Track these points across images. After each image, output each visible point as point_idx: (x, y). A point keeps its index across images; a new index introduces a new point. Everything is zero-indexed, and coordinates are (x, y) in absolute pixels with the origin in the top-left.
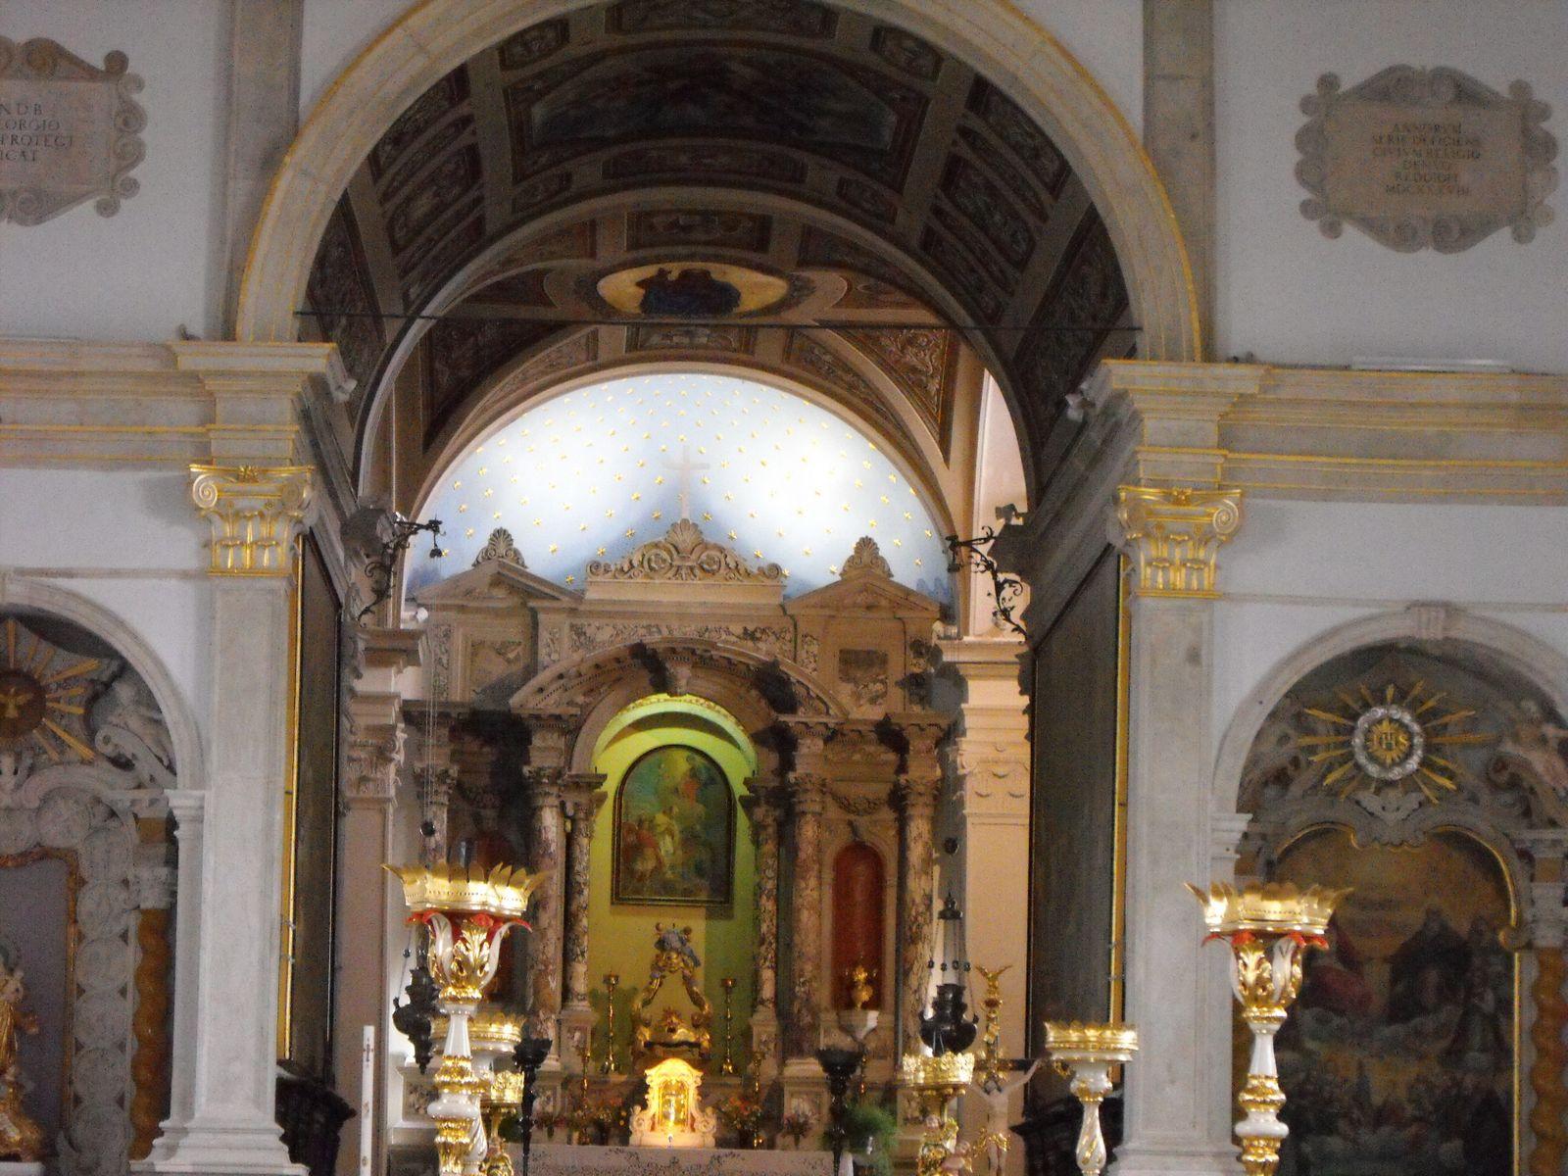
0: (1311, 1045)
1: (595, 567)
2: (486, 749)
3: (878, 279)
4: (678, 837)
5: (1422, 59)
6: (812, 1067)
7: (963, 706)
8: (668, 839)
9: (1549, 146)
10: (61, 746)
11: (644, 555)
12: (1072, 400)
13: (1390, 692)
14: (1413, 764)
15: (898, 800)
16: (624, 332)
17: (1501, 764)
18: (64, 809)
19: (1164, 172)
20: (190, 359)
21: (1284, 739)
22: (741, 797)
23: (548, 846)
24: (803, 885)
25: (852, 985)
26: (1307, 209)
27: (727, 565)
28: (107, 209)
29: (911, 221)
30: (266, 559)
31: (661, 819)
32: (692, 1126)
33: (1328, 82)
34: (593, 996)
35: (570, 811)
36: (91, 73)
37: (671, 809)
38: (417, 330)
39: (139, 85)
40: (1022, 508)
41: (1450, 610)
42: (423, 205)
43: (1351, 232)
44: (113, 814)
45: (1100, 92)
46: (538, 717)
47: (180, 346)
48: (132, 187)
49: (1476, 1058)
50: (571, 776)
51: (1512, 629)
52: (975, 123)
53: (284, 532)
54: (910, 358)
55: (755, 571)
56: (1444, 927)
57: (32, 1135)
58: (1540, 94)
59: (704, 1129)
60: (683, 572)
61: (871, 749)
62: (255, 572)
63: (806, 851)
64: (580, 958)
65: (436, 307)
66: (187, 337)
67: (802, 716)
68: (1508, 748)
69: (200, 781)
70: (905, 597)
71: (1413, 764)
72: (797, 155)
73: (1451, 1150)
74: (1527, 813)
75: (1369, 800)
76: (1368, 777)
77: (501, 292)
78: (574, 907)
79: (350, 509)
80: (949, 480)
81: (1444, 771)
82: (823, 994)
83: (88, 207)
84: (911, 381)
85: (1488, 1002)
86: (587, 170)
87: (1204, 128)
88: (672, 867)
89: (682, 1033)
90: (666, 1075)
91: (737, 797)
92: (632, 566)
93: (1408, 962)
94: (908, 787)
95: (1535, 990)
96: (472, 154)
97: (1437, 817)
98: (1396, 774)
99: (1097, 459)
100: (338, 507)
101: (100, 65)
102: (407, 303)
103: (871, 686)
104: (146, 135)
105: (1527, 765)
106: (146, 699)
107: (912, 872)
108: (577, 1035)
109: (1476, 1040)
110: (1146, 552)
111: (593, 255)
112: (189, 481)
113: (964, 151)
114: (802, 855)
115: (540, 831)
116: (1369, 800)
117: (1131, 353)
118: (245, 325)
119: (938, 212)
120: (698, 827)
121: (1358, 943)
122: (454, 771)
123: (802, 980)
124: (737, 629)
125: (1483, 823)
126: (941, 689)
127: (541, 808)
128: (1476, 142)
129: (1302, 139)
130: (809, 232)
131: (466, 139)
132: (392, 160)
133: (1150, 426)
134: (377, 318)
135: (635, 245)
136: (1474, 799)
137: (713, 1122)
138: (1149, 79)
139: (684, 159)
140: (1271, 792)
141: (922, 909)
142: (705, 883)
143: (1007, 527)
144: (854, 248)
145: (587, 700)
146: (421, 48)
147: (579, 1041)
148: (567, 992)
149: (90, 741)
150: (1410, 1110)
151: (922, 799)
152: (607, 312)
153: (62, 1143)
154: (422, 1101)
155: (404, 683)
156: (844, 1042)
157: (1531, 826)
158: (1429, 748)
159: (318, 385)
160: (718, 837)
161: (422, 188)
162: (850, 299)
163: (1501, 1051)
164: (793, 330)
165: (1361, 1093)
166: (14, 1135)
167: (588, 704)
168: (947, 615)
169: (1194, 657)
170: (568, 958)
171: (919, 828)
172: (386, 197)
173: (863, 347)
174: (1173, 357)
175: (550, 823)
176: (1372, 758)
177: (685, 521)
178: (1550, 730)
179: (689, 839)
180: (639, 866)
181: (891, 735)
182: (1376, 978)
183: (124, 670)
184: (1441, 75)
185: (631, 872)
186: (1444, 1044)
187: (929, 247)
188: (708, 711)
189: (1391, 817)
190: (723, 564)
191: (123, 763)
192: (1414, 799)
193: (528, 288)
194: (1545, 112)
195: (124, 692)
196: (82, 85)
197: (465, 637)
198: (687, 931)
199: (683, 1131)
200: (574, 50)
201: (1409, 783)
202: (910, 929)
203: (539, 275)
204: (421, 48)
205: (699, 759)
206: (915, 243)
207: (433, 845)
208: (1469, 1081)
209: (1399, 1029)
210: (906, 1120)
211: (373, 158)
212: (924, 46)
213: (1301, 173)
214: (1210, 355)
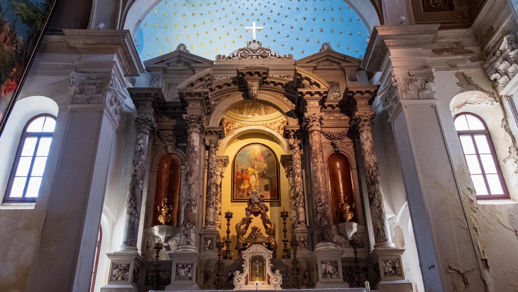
1: (219, 57)
2: (172, 120)
4: (257, 175)
7: (390, 57)
8: (253, 176)
11: (238, 53)
22: (282, 156)
23: (193, 147)
24: (316, 160)
27: (272, 55)
31: (250, 170)
32: (268, 280)
35: (208, 143)
37: (254, 166)
46: (191, 95)
50: (208, 128)
55: (283, 56)
59: (276, 283)
60: (254, 57)
61: (337, 115)
64: (211, 206)
78: (209, 184)
88: (255, 187)
90: (252, 253)
91: (279, 159)
92: (234, 56)
94: (360, 118)
103: (334, 93)
107: (367, 153)
108: (209, 242)
114: (314, 148)
115: (190, 142)
120: (265, 172)
123: (320, 204)
127: (191, 133)
137: (280, 278)
141: (374, 169)
142: (268, 193)
145: (216, 103)
147: (210, 245)
151: (366, 123)
154: (120, 273)
160: (274, 175)
167: (216, 104)
175: (195, 139)
177: (254, 41)
179: (262, 176)
180: (242, 187)
185: (240, 189)
188: (267, 128)
190: (270, 55)
197: (166, 82)
199: (263, 284)
202: (370, 178)
205: (264, 148)
207: (139, 149)
210: (385, 273)
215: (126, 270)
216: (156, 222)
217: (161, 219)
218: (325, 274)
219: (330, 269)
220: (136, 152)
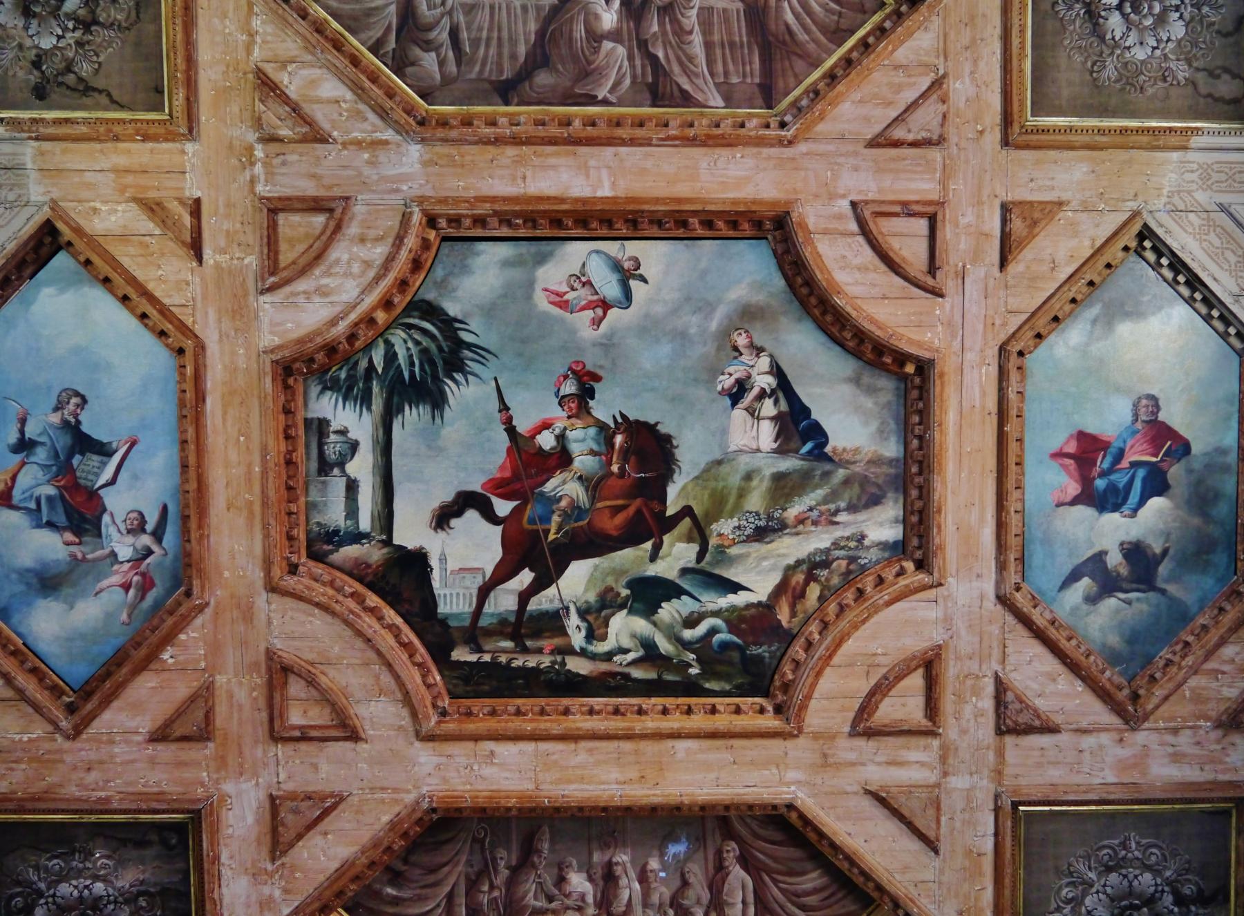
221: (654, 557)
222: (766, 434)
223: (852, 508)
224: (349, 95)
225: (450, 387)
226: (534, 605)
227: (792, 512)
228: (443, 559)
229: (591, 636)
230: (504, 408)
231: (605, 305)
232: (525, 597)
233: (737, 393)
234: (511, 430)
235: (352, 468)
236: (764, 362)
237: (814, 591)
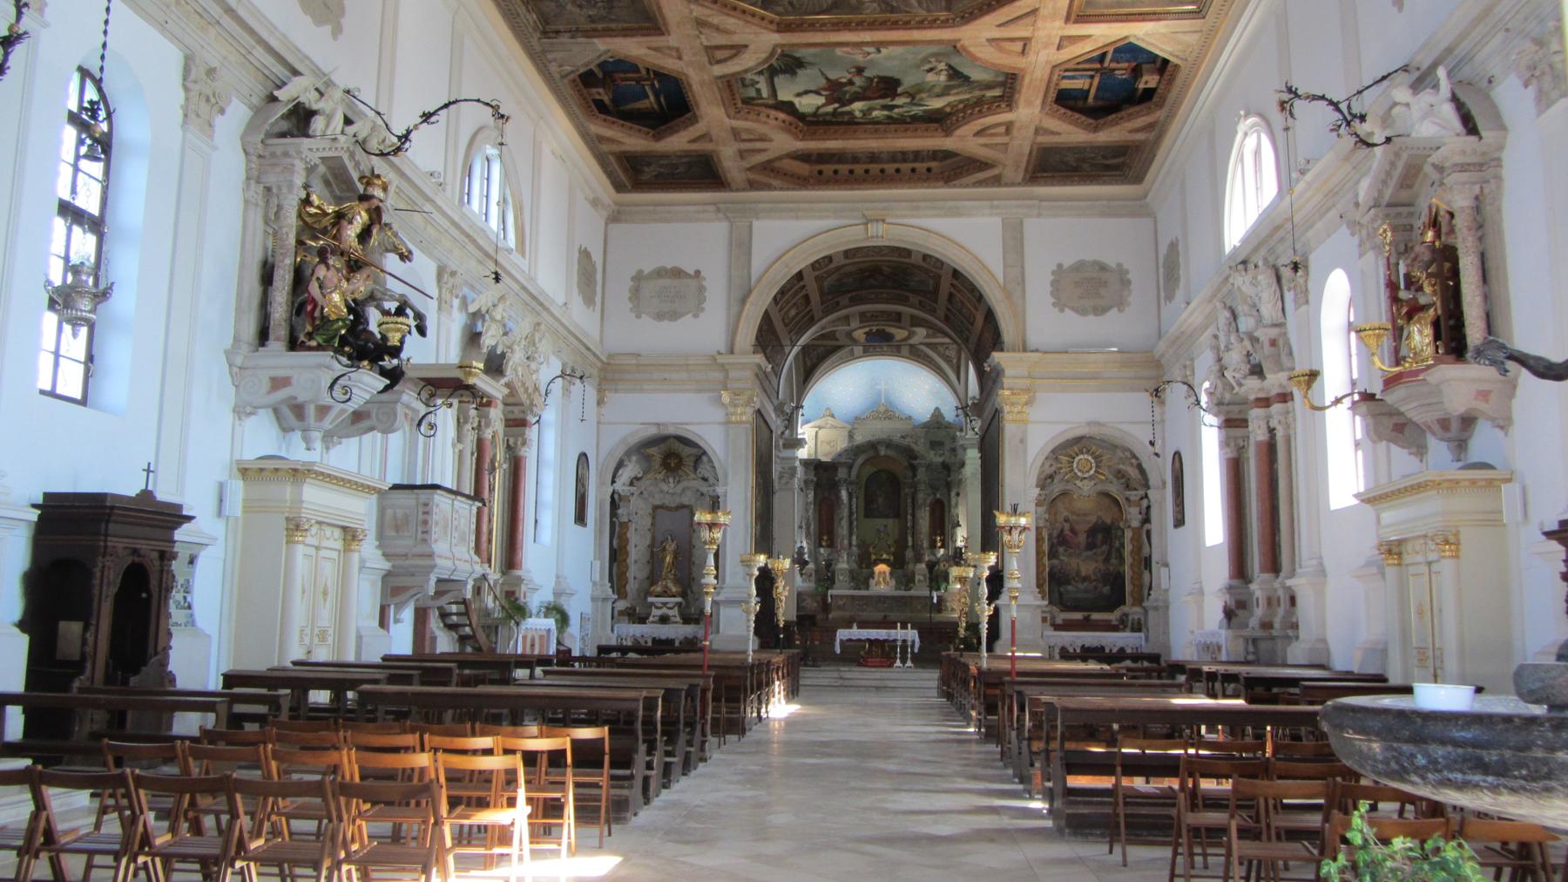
0: (1062, 558)
3: (934, 330)
5: (1088, 256)
6: (923, 566)
9: (1129, 282)
10: (687, 475)
12: (985, 365)
13: (1085, 450)
14: (1092, 472)
15: (949, 486)
16: (861, 348)
17: (1119, 471)
18: (689, 493)
19: (1008, 296)
20: (720, 360)
21: (1051, 465)
25: (935, 541)
26: (1054, 305)
28: (696, 316)
29: (941, 312)
30: (744, 418)
33: (1060, 266)
34: (858, 546)
36: (690, 276)
38: (796, 350)
39: (705, 279)
40: (978, 397)
41: (1099, 424)
42: (793, 312)
43: (1067, 310)
44: (702, 494)
45: (989, 272)
47: (718, 357)
48: (703, 310)
49: (1113, 561)
51: (1121, 430)
52: (955, 282)
53: (750, 411)
54: (947, 353)
56: (1103, 523)
57: (680, 590)
58: (1125, 267)
62: (741, 422)
63: (920, 501)
65: (803, 340)
66: (719, 353)
67: (918, 461)
68: (1121, 466)
69: (726, 484)
70: (948, 426)
71: (1092, 472)
72: (907, 294)
73: (1106, 590)
74: (1128, 486)
75: (1078, 483)
76: (1077, 477)
77: (823, 337)
79: (776, 402)
80: (960, 389)
81: (1102, 474)
82: (926, 544)
83: (690, 315)
84: (947, 360)
85: (1117, 544)
86: (844, 300)
87: (1022, 282)
89: (885, 556)
93: (1092, 531)
95: (1132, 540)
96: (807, 297)
97: (1100, 488)
98: (1086, 475)
99: (994, 382)
100: (772, 402)
101: (693, 274)
102: (792, 342)
104: (706, 294)
105: (1126, 472)
106: (710, 461)
109: (1114, 555)
110: (1007, 409)
111: (849, 325)
112: (721, 396)
113: (954, 292)
116: (1078, 483)
117: (1002, 350)
118: (737, 349)
119: (948, 309)
121: (1077, 528)
122: (815, 479)
124: (899, 435)
125: (1115, 489)
126: (960, 451)
128: (1106, 282)
129: (1053, 283)
130: (912, 317)
131: (804, 292)
132: (781, 299)
133: (1008, 372)
134: (782, 346)
135: (861, 322)
136: (1111, 482)
138: (1005, 267)
139: (873, 296)
140: (1049, 481)
143: (973, 404)
144: (927, 321)
146: (787, 266)
148: (850, 544)
149: (695, 473)
150: (1093, 577)
152: (855, 342)
153: (689, 592)
155: (803, 453)
156: (933, 558)
157: (1130, 490)
158: (1097, 466)
159: (759, 366)
161: (792, 307)
162: (928, 336)
163: (1121, 559)
164: (911, 346)
165: (1078, 573)
166: (674, 590)
168: (961, 430)
169: (1022, 441)
170: (851, 534)
171: (953, 494)
172: (780, 311)
173: (932, 349)
174: (1014, 351)
175: (844, 494)
176: (1080, 470)
178: (1134, 461)
181: (946, 467)
182: (1082, 538)
183: (704, 453)
184: (1096, 263)
186: (1103, 557)
187: (947, 319)
189: (1086, 488)
191: (705, 479)
192: (1093, 483)
193: (831, 336)
194: (1127, 272)
195: (704, 458)
196: (689, 280)
198: (886, 526)
200: (832, 266)
201: (1091, 478)
203: (835, 331)
204: (787, 266)
206: (943, 318)
208: (1111, 568)
209: (1089, 553)
211: (775, 298)
212: (938, 260)
213: (1052, 293)
214: (1025, 350)
215: (811, 575)
216: (821, 546)
217: (824, 544)
218: (919, 581)
219: (922, 578)
220: (807, 504)
221: (892, 100)
222: (943, 78)
223: (981, 90)
224: (741, 23)
225: (798, 71)
226: (840, 110)
227: (953, 92)
228: (800, 103)
229: (864, 115)
230: (822, 73)
231: (869, 54)
232: (835, 109)
233: (931, 70)
234: (827, 78)
235: (758, 86)
236: (943, 64)
237: (961, 106)
